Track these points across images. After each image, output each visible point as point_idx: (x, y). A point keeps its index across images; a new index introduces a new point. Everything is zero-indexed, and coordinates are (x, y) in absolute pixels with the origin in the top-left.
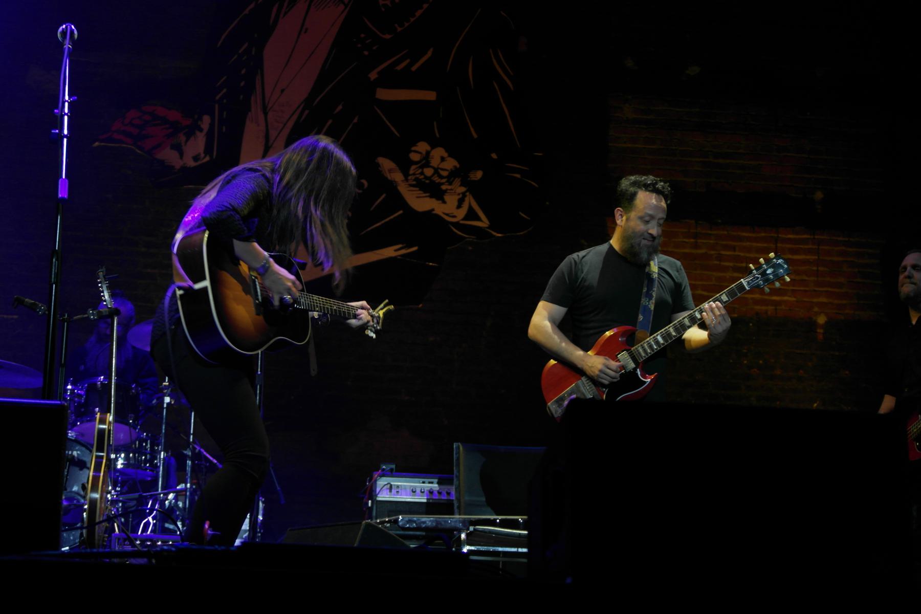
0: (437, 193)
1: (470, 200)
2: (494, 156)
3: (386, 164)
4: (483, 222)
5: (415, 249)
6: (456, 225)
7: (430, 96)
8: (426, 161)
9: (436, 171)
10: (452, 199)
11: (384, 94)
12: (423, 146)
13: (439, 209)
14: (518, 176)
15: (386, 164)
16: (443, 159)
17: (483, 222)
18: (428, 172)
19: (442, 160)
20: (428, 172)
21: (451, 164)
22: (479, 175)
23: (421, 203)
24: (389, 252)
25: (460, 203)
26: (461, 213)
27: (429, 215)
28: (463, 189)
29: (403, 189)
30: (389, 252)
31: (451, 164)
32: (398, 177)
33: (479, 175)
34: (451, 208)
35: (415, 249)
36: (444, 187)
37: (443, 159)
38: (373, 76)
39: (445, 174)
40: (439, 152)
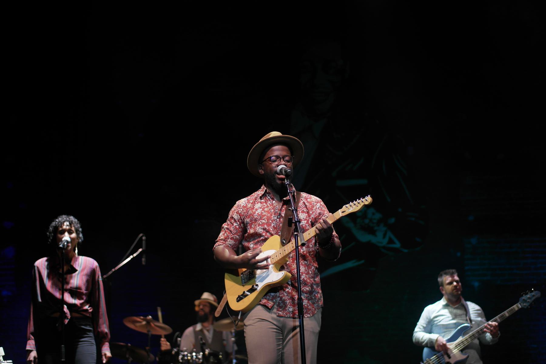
0: (371, 231)
1: (390, 234)
2: (400, 210)
4: (397, 245)
5: (362, 262)
6: (384, 247)
9: (371, 220)
10: (380, 235)
14: (413, 219)
16: (373, 214)
17: (397, 245)
18: (367, 221)
20: (367, 221)
21: (378, 216)
22: (392, 220)
23: (364, 237)
24: (350, 264)
25: (385, 235)
26: (385, 242)
27: (369, 244)
28: (384, 229)
30: (350, 264)
31: (378, 216)
33: (392, 220)
34: (380, 238)
35: (362, 262)
36: (376, 228)
37: (373, 214)
39: (375, 221)
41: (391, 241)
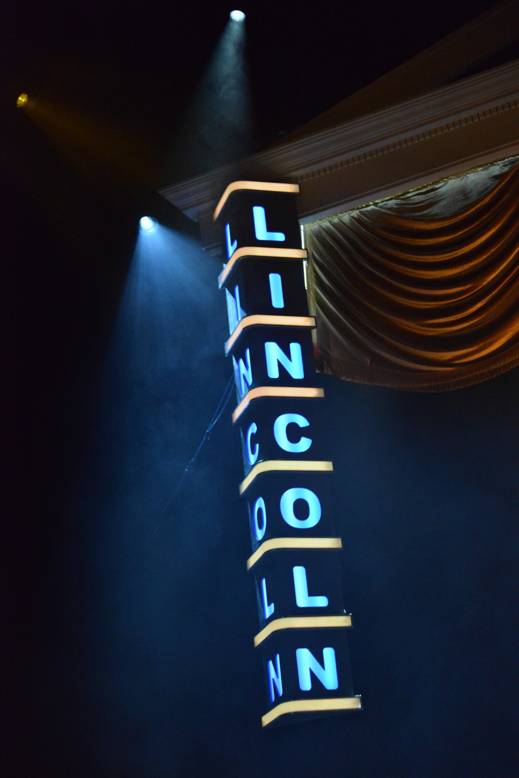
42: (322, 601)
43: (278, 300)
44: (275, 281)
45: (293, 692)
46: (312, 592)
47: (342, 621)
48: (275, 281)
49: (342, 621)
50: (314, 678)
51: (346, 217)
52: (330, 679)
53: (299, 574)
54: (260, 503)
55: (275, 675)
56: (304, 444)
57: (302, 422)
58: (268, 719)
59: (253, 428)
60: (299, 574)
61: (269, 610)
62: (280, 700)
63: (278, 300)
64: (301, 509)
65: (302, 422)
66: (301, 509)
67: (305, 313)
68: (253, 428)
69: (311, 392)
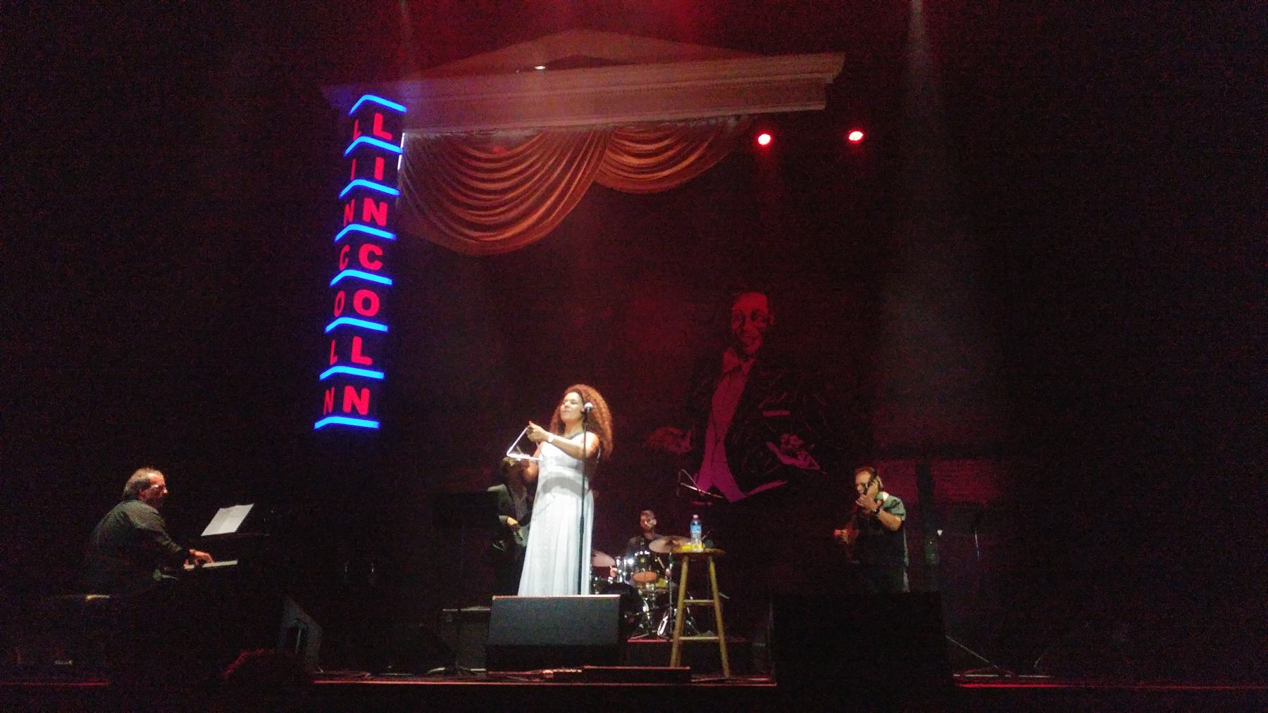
0: (795, 456)
3: (769, 444)
7: (786, 413)
8: (788, 442)
11: (765, 413)
12: (786, 436)
13: (796, 462)
15: (769, 444)
17: (818, 468)
19: (795, 441)
23: (787, 461)
29: (779, 456)
32: (776, 450)
34: (801, 462)
38: (760, 406)
40: (793, 438)
41: (811, 465)
42: (369, 361)
43: (379, 173)
44: (380, 162)
45: (338, 411)
46: (363, 354)
47: (378, 375)
48: (380, 162)
49: (378, 375)
50: (354, 407)
51: (432, 136)
52: (363, 407)
53: (357, 342)
54: (341, 295)
55: (329, 399)
56: (378, 265)
57: (379, 252)
58: (319, 425)
59: (346, 249)
60: (357, 342)
61: (333, 359)
62: (329, 415)
63: (379, 173)
64: (367, 303)
65: (379, 252)
66: (367, 303)
67: (394, 187)
68: (346, 249)
69: (388, 235)
